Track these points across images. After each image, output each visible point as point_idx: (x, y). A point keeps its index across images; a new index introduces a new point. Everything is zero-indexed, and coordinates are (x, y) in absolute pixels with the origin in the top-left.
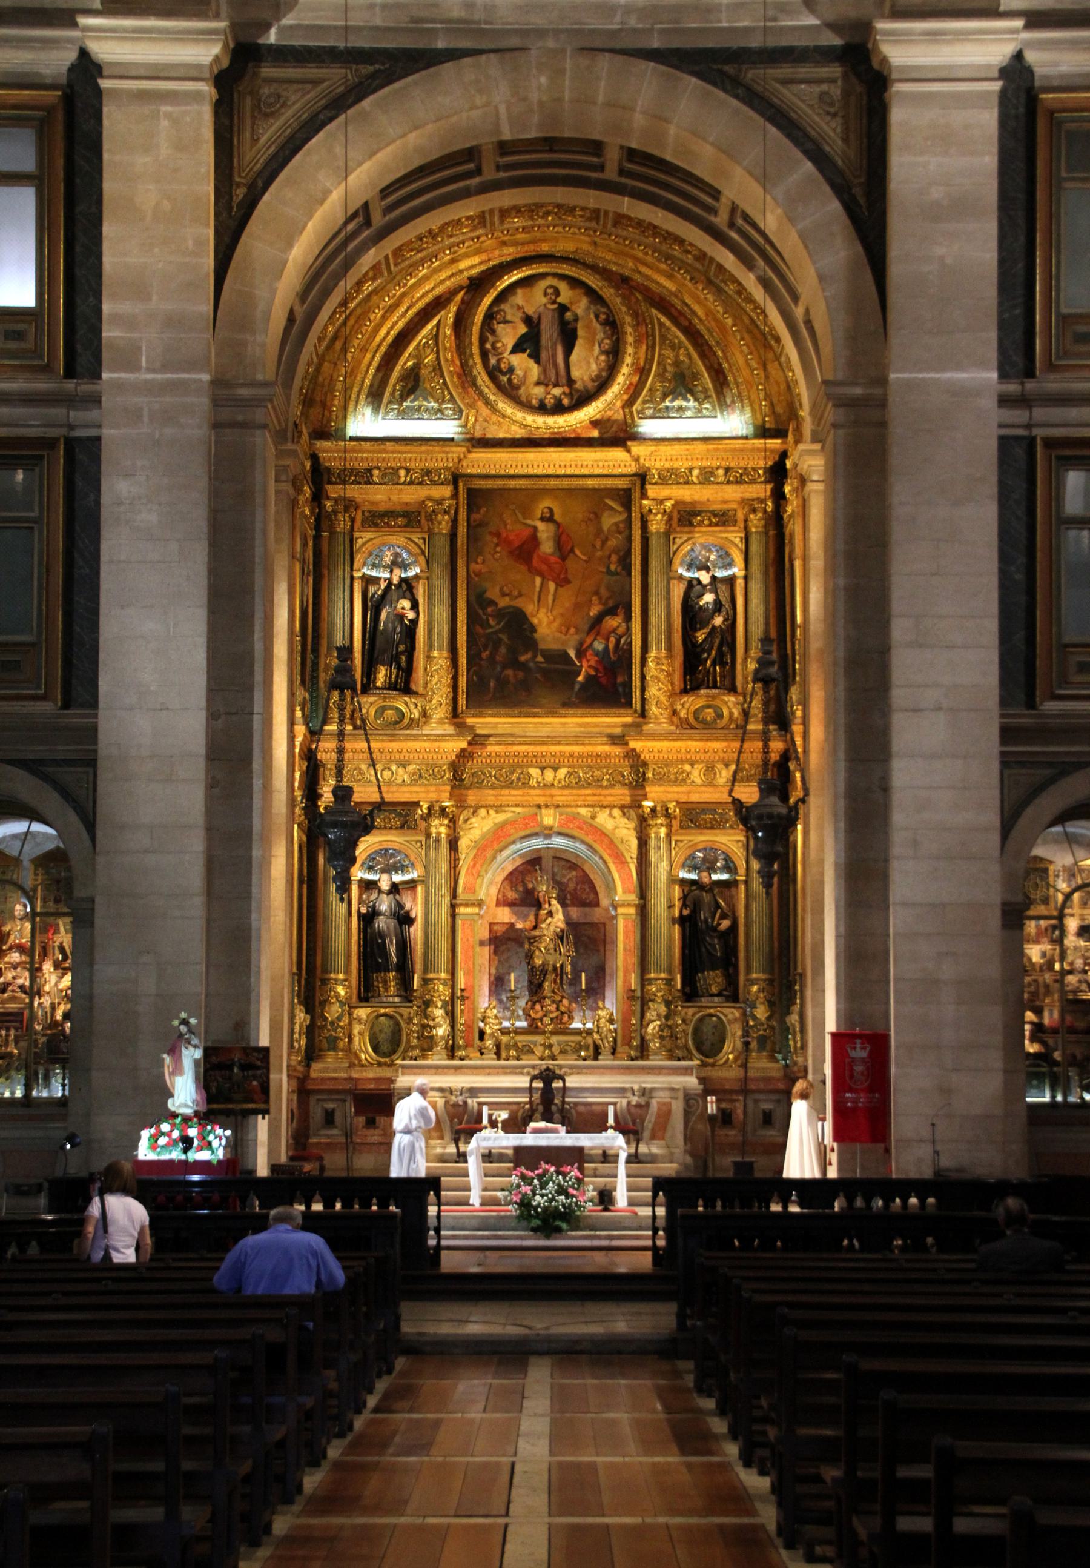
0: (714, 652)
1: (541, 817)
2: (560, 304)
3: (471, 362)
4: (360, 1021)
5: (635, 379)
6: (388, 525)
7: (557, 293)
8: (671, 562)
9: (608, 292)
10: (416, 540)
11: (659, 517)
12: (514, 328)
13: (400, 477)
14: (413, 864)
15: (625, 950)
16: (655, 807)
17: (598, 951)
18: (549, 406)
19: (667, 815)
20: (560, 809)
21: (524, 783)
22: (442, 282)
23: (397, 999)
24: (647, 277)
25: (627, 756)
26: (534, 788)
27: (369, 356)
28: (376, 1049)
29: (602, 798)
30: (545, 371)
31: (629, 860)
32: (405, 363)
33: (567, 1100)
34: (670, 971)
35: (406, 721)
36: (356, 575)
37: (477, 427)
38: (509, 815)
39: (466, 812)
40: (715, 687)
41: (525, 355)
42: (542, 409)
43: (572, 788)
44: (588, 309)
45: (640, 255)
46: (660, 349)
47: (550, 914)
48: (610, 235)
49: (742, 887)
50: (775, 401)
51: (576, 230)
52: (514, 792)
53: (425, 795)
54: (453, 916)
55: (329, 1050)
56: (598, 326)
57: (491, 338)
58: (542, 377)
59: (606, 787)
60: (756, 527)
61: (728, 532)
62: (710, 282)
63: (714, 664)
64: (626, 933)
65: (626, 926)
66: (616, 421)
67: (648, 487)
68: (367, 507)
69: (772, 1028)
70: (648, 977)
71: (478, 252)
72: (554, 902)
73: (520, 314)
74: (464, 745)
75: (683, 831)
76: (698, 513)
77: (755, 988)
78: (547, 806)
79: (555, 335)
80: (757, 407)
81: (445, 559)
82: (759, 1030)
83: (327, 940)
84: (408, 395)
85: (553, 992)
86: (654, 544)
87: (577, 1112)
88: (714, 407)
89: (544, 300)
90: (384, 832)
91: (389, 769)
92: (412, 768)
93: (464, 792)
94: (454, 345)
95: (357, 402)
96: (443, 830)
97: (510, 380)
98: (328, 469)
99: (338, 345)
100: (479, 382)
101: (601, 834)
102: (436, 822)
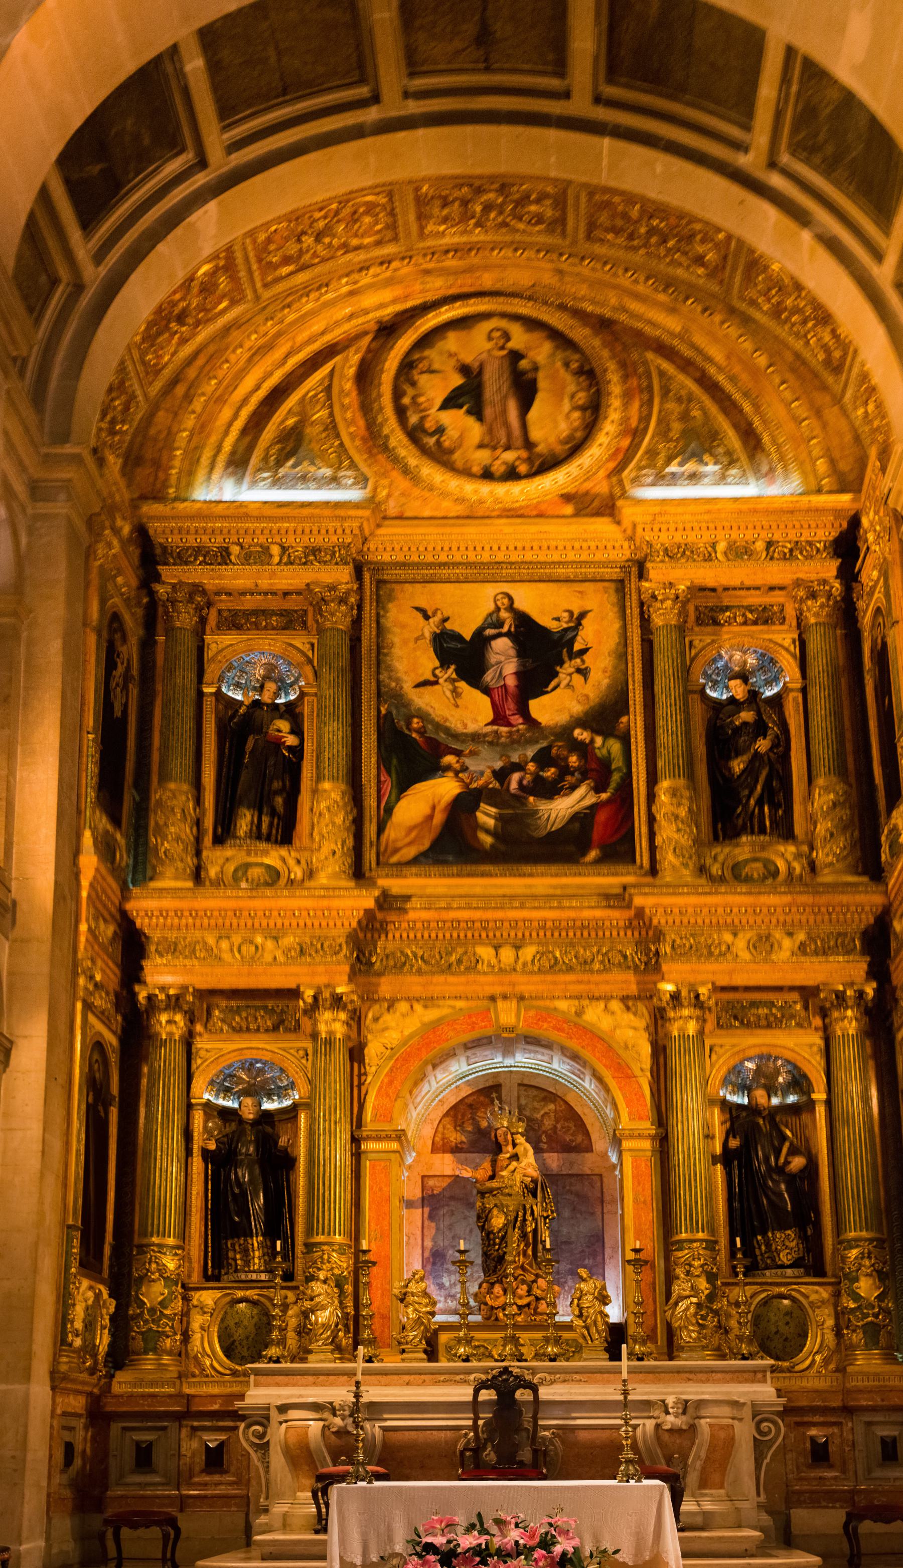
0: (759, 788)
3: (380, 419)
4: (202, 1309)
5: (626, 443)
6: (257, 627)
7: (507, 336)
8: (688, 671)
9: (579, 333)
10: (300, 645)
11: (669, 603)
14: (293, 1083)
15: (636, 1201)
17: (593, 1214)
18: (498, 474)
20: (527, 1002)
22: (338, 323)
23: (263, 1277)
24: (639, 317)
25: (629, 925)
26: (485, 973)
27: (226, 413)
29: (592, 987)
30: (490, 431)
31: (638, 1072)
32: (283, 421)
34: (713, 1231)
35: (283, 881)
36: (208, 690)
37: (392, 503)
38: (445, 1011)
39: (376, 1007)
40: (762, 831)
42: (487, 475)
43: (545, 973)
44: (552, 355)
46: (661, 403)
49: (820, 1111)
50: (837, 454)
52: (451, 979)
54: (357, 1156)
55: (146, 1353)
56: (568, 378)
57: (410, 392)
59: (599, 972)
60: (816, 615)
61: (773, 632)
62: (732, 311)
63: (760, 803)
65: (636, 1167)
66: (597, 496)
67: (649, 565)
68: (224, 603)
69: (887, 1312)
70: (677, 1238)
71: (389, 282)
72: (520, 1139)
73: (453, 362)
75: (723, 1032)
76: (728, 608)
77: (854, 1253)
78: (505, 997)
79: (505, 388)
80: (809, 468)
81: (343, 661)
82: (867, 1315)
83: (148, 1187)
84: (287, 458)
85: (523, 1268)
86: (663, 643)
87: (563, 1442)
88: (744, 474)
89: (489, 345)
90: (246, 1036)
91: (251, 942)
92: (289, 940)
93: (374, 980)
96: (339, 1029)
97: (438, 442)
100: (393, 443)
101: (592, 1035)
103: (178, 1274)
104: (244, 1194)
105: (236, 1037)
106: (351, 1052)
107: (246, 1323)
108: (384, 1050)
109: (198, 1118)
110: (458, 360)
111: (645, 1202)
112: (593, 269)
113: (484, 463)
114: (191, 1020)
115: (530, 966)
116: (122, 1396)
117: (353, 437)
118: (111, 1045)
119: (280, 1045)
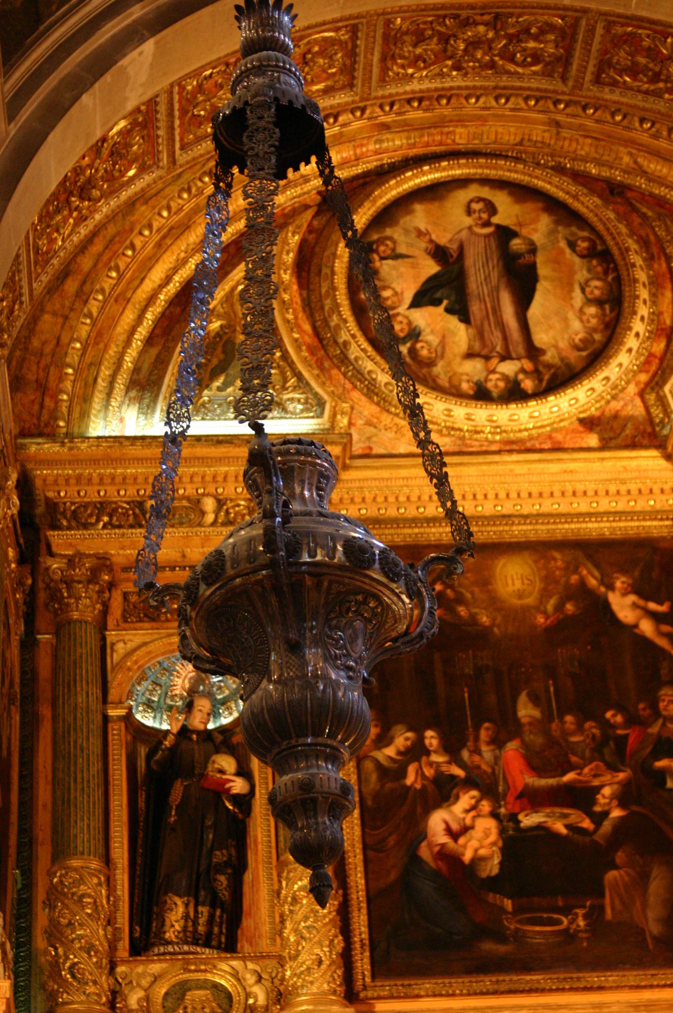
2: (498, 227)
7: (491, 209)
12: (414, 266)
13: (203, 513)
18: (495, 393)
27: (129, 316)
30: (481, 335)
41: (441, 309)
42: (482, 395)
44: (552, 232)
45: (645, 138)
48: (584, 108)
51: (521, 102)
56: (577, 260)
58: (477, 346)
66: (630, 418)
73: (423, 245)
79: (495, 275)
84: (213, 376)
89: (468, 221)
94: (298, 299)
95: (109, 394)
97: (413, 351)
98: (52, 506)
99: (71, 286)
100: (354, 352)
110: (431, 241)
112: (597, 121)
113: (475, 379)
117: (298, 349)
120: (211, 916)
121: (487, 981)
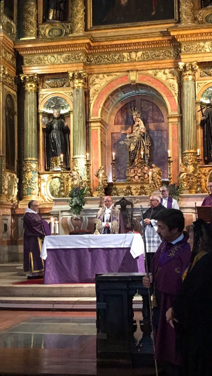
1: (130, 77)
15: (173, 139)
16: (185, 65)
19: (193, 70)
20: (139, 72)
21: (121, 60)
26: (126, 62)
28: (52, 193)
29: (160, 64)
31: (174, 95)
33: (134, 215)
43: (145, 61)
47: (138, 125)
52: (116, 65)
53: (70, 69)
55: (28, 195)
59: (162, 59)
64: (173, 131)
65: (173, 128)
70: (184, 152)
74: (88, 41)
78: (132, 71)
92: (64, 55)
93: (93, 67)
102: (77, 81)
103: (36, 169)
104: (55, 142)
105: (51, 89)
106: (85, 92)
107: (57, 184)
108: (95, 91)
109: (41, 116)
111: (176, 140)
114: (38, 85)
115: (140, 59)
116: (21, 209)
118: (14, 94)
119: (64, 92)
120: (60, 13)
121: (116, 26)
